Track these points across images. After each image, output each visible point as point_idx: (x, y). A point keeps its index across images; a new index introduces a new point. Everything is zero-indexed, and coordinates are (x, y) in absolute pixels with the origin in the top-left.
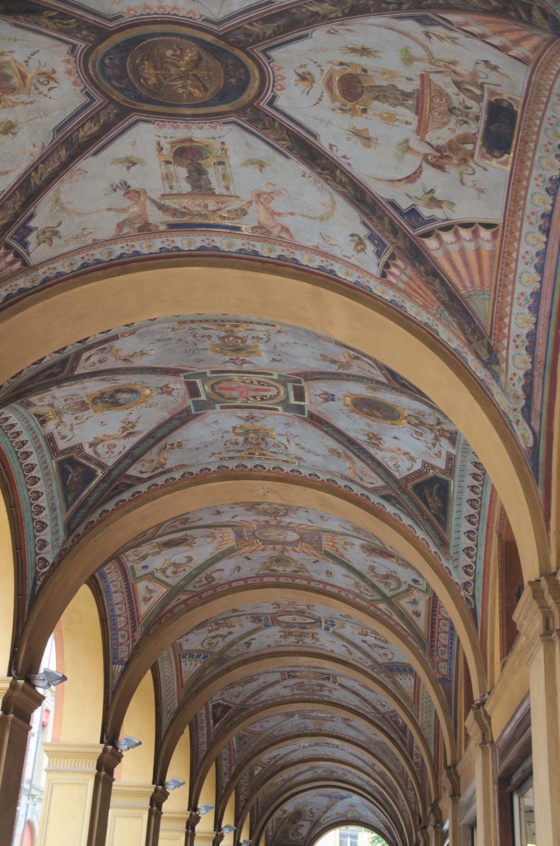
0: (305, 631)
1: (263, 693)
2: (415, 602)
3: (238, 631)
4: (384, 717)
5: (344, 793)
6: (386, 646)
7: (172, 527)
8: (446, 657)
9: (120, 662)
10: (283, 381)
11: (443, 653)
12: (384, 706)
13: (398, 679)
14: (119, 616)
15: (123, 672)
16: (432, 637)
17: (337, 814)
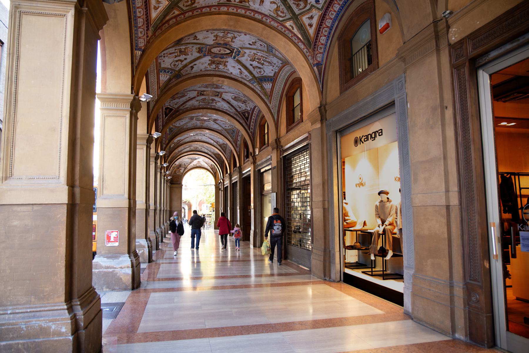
0: (222, 60)
1: (187, 103)
2: (311, 18)
3: (190, 58)
4: (239, 113)
5: (197, 156)
6: (261, 67)
8: (322, 51)
9: (139, 49)
11: (321, 48)
12: (240, 108)
13: (264, 85)
14: (139, 17)
15: (142, 56)
16: (316, 39)
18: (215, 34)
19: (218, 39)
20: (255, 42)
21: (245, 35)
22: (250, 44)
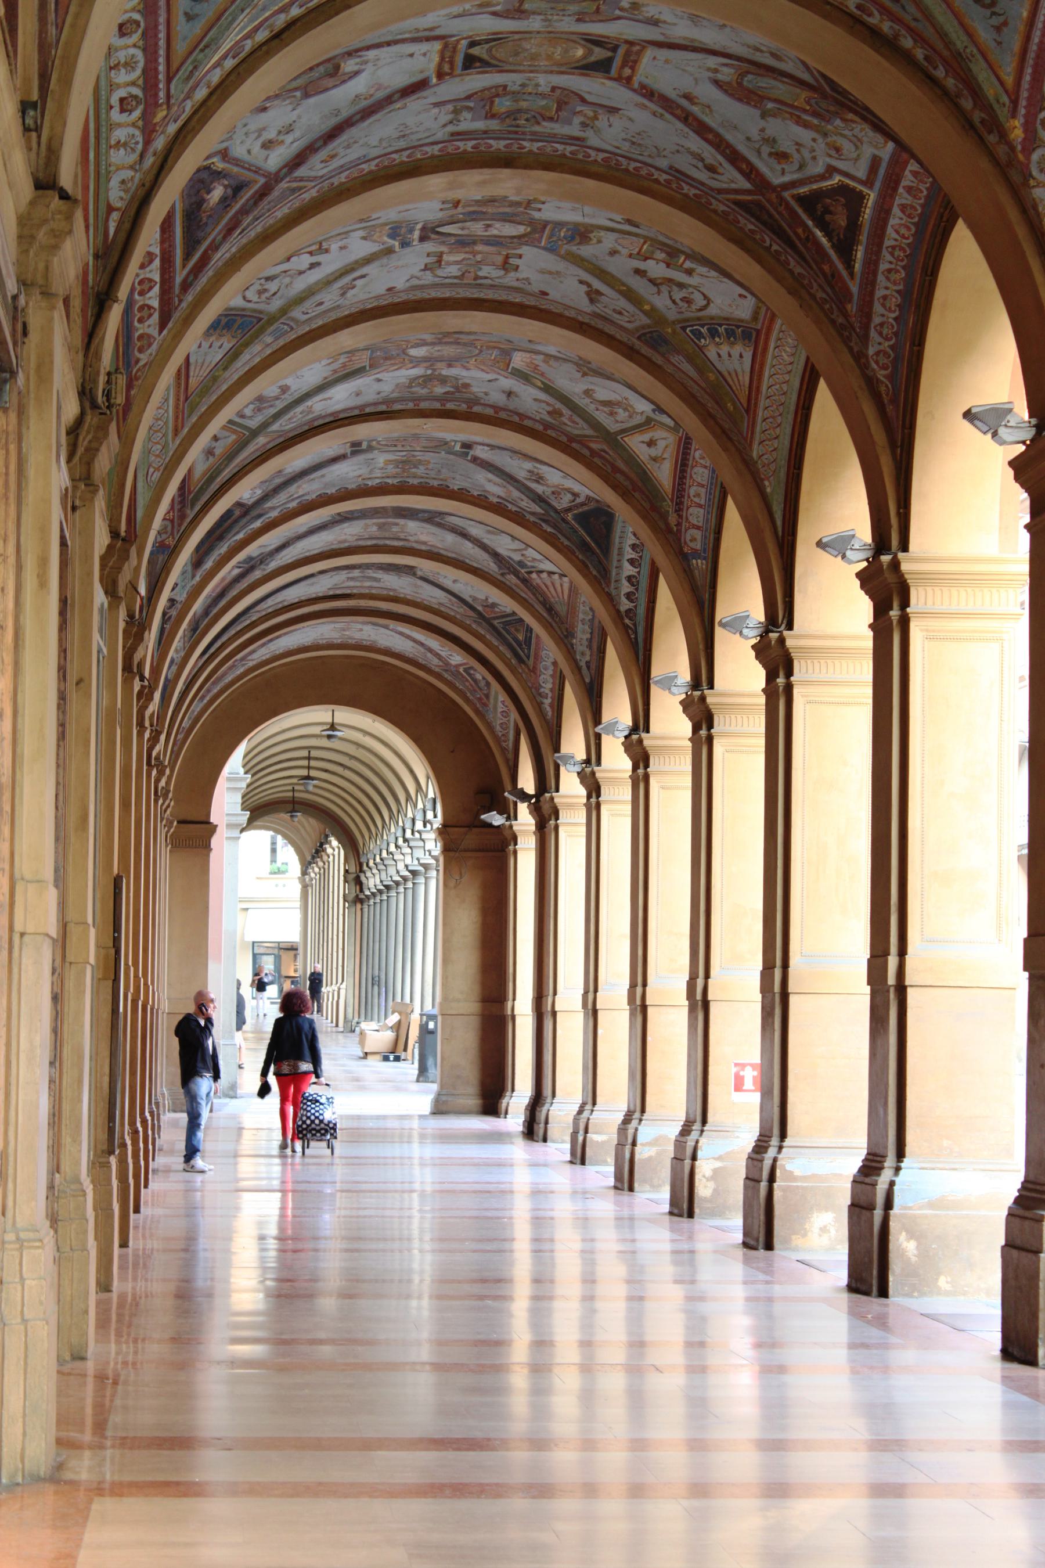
7: (574, 422)
10: (370, 448)
18: (512, 274)
19: (499, 259)
20: (343, 294)
21: (390, 289)
22: (363, 276)
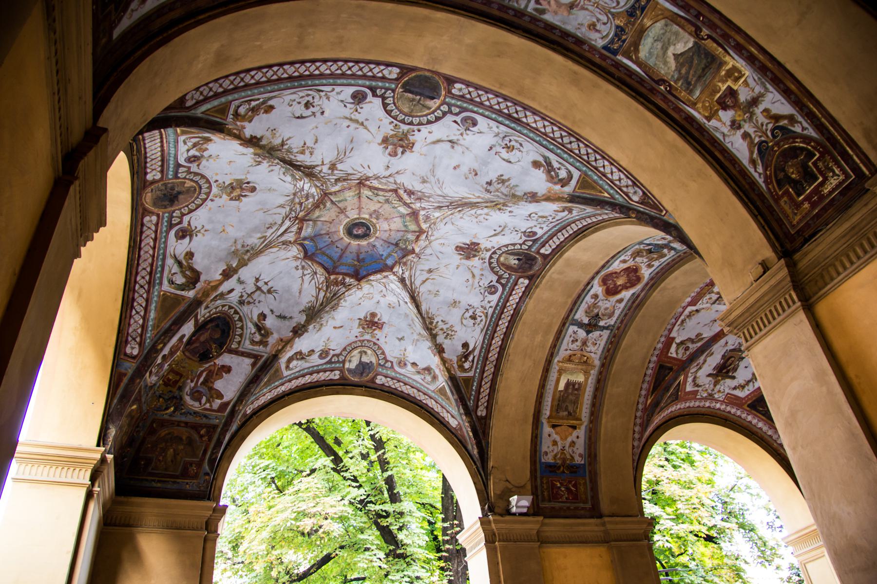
17: (324, 354)
